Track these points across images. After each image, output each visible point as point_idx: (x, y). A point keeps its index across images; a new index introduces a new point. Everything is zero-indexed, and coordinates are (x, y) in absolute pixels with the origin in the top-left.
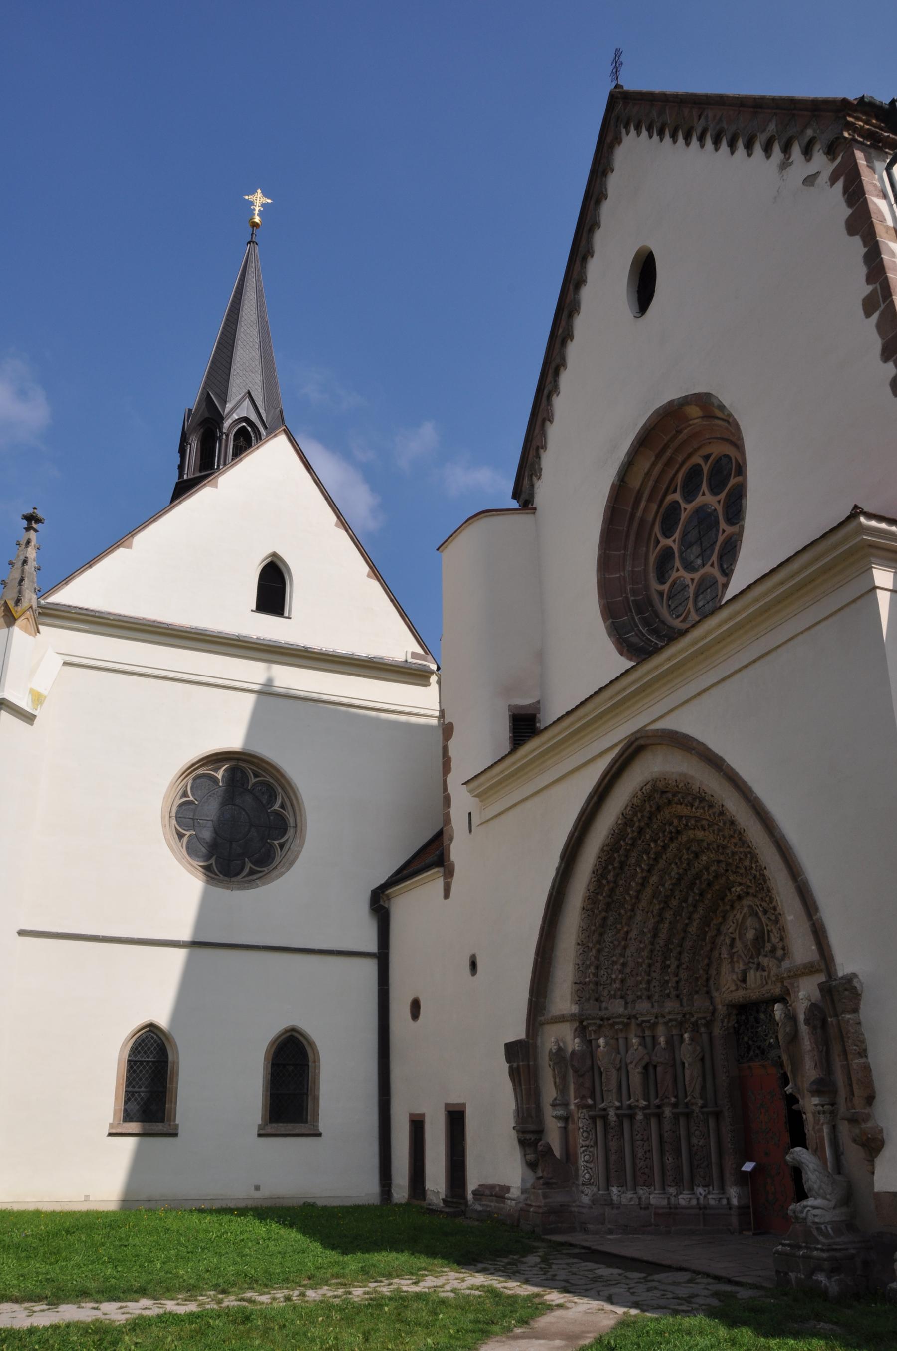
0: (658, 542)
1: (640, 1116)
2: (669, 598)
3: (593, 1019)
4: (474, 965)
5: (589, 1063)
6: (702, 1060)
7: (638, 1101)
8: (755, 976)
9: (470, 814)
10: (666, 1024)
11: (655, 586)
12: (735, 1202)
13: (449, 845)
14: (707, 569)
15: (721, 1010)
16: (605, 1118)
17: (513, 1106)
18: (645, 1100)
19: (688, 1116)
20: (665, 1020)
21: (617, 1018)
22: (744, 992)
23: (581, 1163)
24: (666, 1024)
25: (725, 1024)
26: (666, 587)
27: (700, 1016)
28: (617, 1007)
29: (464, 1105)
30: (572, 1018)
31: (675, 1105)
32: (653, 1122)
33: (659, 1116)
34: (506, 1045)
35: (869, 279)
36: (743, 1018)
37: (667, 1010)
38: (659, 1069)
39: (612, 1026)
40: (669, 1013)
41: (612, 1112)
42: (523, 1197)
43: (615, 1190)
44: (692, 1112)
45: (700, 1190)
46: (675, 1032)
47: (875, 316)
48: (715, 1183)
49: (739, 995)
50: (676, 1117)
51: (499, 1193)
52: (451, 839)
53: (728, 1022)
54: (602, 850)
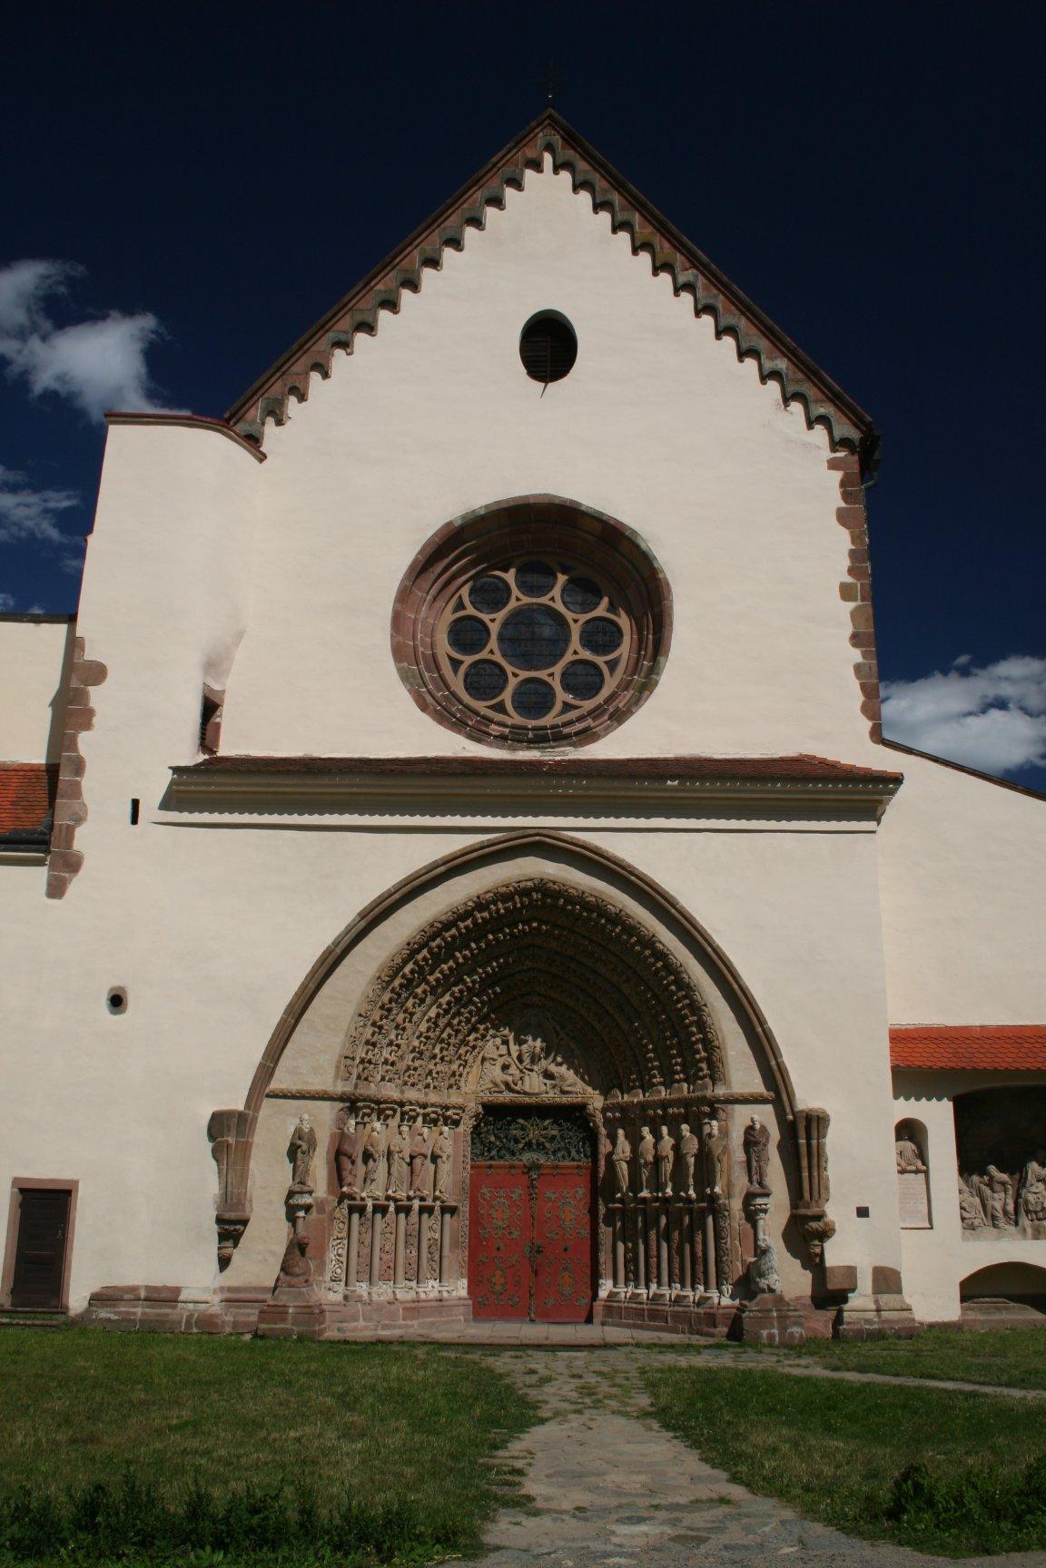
0: (460, 606)
1: (392, 1209)
2: (467, 675)
4: (117, 1001)
9: (135, 803)
10: (425, 1116)
11: (444, 648)
12: (463, 1293)
13: (70, 832)
14: (542, 674)
15: (473, 1107)
17: (213, 1187)
23: (331, 1255)
26: (468, 660)
28: (391, 1091)
29: (76, 1183)
30: (341, 1099)
31: (422, 1199)
32: (402, 1216)
33: (407, 1210)
35: (851, 571)
38: (418, 1161)
39: (380, 1113)
41: (370, 1203)
42: (217, 1299)
43: (364, 1285)
45: (431, 1282)
47: (852, 605)
48: (445, 1276)
49: (507, 1097)
50: (422, 1210)
51: (169, 1296)
52: (79, 819)
54: (432, 925)
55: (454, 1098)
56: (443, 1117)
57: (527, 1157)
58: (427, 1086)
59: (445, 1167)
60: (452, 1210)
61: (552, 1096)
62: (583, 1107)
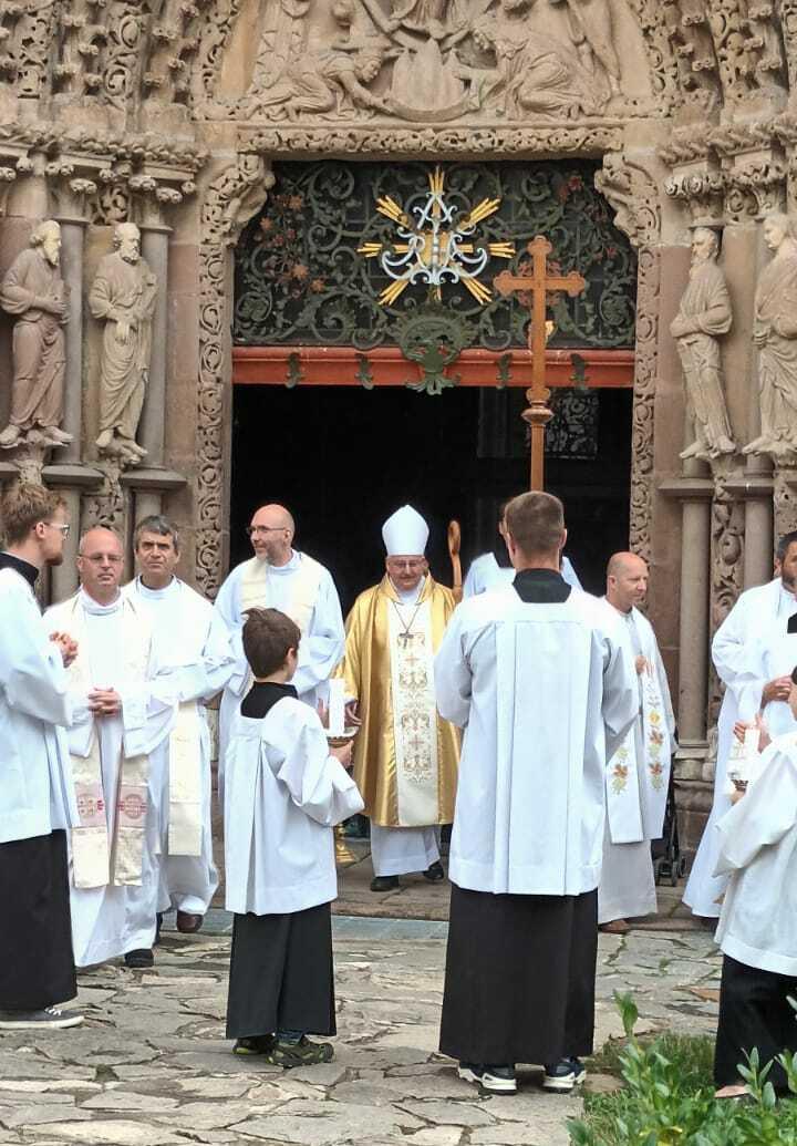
8: (436, 77)
10: (56, 183)
15: (234, 165)
20: (55, 167)
22: (364, 119)
24: (56, 183)
25: (229, 214)
27: (165, 174)
31: (53, 455)
36: (296, 203)
37: (75, 134)
40: (78, 147)
44: (101, 482)
46: (71, 213)
49: (339, 130)
53: (241, 207)
55: (159, 127)
56: (115, 189)
57: (408, 326)
58: (59, 83)
59: (121, 353)
60: (171, 494)
61: (498, 127)
62: (586, 163)
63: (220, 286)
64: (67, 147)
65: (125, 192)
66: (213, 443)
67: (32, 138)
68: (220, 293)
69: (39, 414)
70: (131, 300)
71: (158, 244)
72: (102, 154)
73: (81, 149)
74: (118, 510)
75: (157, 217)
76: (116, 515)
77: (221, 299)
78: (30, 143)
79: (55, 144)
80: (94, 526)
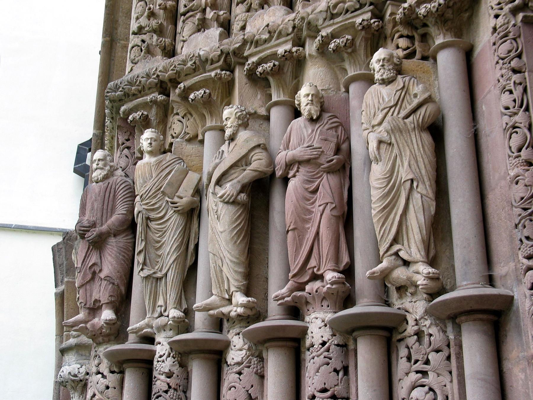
1: (237, 352)
3: (141, 92)
5: (121, 210)
6: (436, 130)
7: (230, 301)
16: (145, 364)
18: (247, 294)
19: (388, 333)
21: (195, 70)
33: (294, 345)
34: (53, 248)
40: (331, 15)
63: (514, 64)
64: (321, 21)
65: (405, 32)
66: (528, 238)
67: (287, 29)
68: (515, 71)
69: (313, 263)
70: (380, 116)
71: (447, 62)
72: (356, 10)
73: (333, 16)
74: (437, 351)
75: (442, 36)
76: (432, 356)
77: (516, 78)
78: (288, 35)
79: (309, 23)
80: (407, 374)
